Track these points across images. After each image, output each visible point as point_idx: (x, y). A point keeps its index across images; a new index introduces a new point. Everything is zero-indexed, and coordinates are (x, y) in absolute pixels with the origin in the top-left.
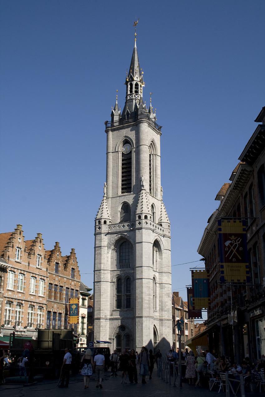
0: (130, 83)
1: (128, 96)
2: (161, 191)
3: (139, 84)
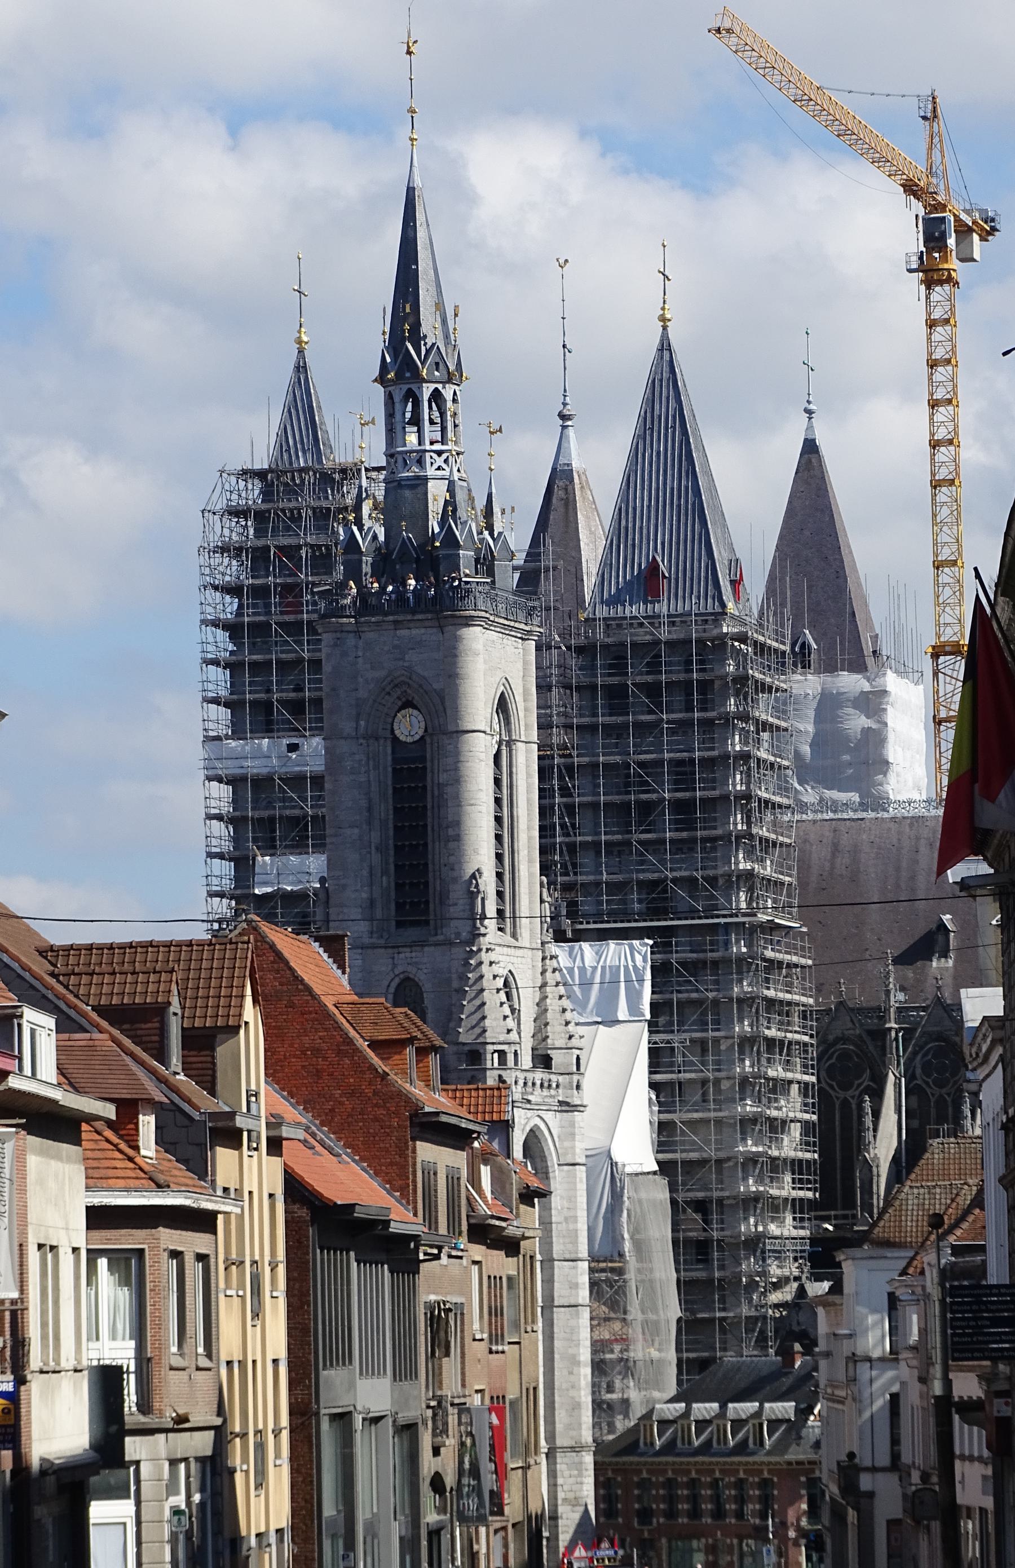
2: (542, 901)
3: (448, 392)
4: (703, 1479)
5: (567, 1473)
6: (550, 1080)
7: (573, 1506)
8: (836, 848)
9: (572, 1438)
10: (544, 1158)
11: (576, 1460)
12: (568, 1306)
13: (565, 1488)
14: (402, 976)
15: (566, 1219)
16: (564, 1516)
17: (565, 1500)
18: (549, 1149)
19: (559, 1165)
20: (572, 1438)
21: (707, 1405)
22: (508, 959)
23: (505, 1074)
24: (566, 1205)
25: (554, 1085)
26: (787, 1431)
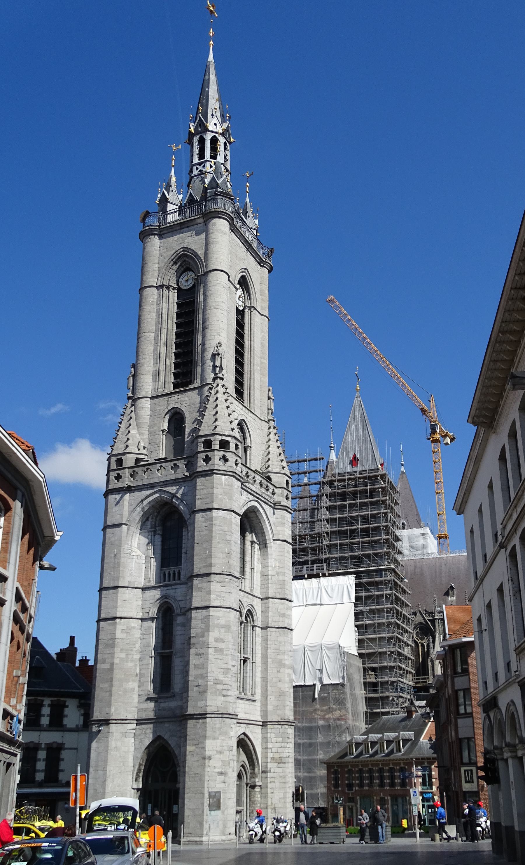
0: (198, 137)
1: (195, 168)
4: (374, 768)
5: (274, 740)
6: (267, 486)
7: (279, 763)
8: (415, 567)
9: (278, 715)
10: (263, 534)
11: (281, 731)
12: (278, 628)
13: (273, 750)
14: (172, 411)
15: (278, 573)
16: (272, 771)
17: (273, 759)
18: (267, 527)
19: (274, 540)
20: (278, 715)
21: (376, 735)
22: (243, 413)
23: (228, 456)
24: (277, 564)
25: (271, 491)
26: (412, 744)
